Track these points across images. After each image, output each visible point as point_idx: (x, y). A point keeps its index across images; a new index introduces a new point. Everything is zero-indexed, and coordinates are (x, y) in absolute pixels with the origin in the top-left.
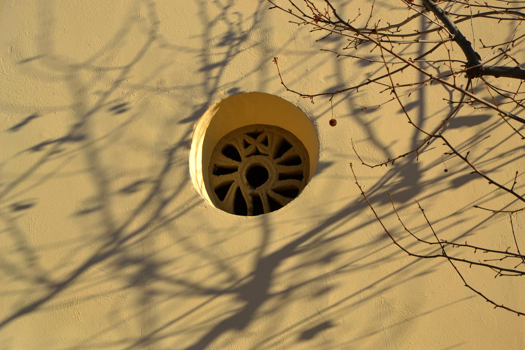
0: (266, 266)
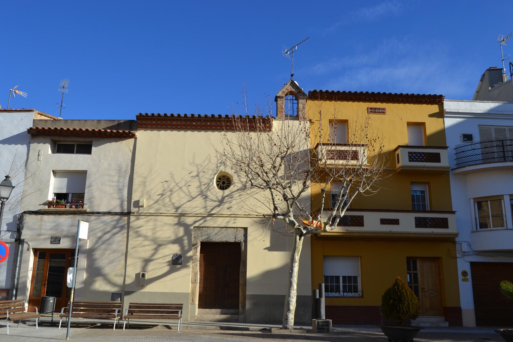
0: (223, 198)
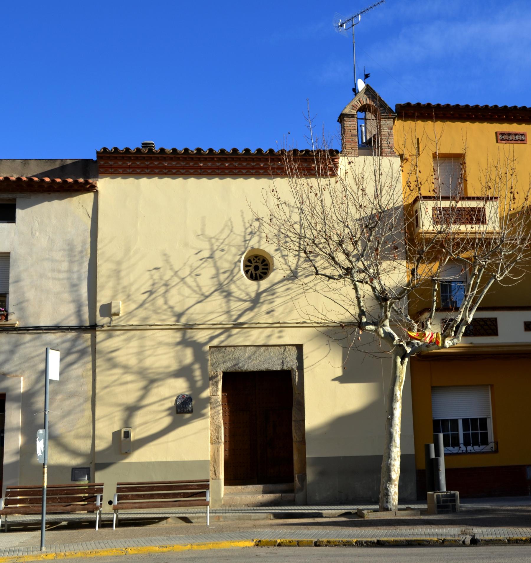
0: (259, 295)
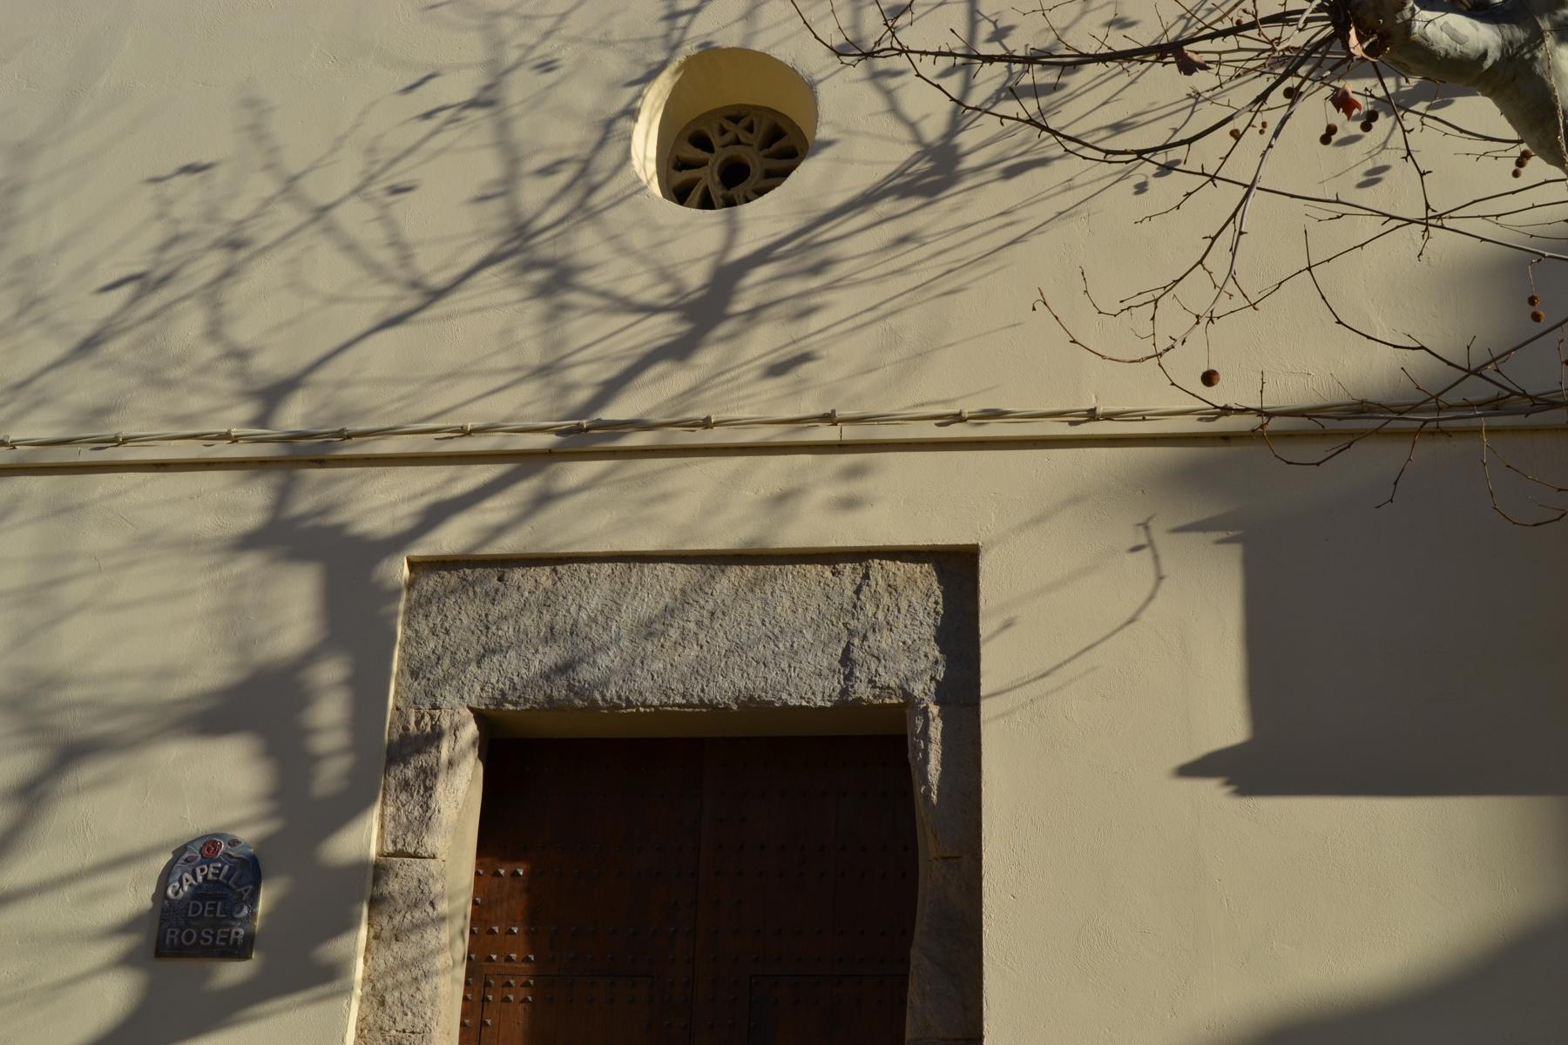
0: (726, 277)
